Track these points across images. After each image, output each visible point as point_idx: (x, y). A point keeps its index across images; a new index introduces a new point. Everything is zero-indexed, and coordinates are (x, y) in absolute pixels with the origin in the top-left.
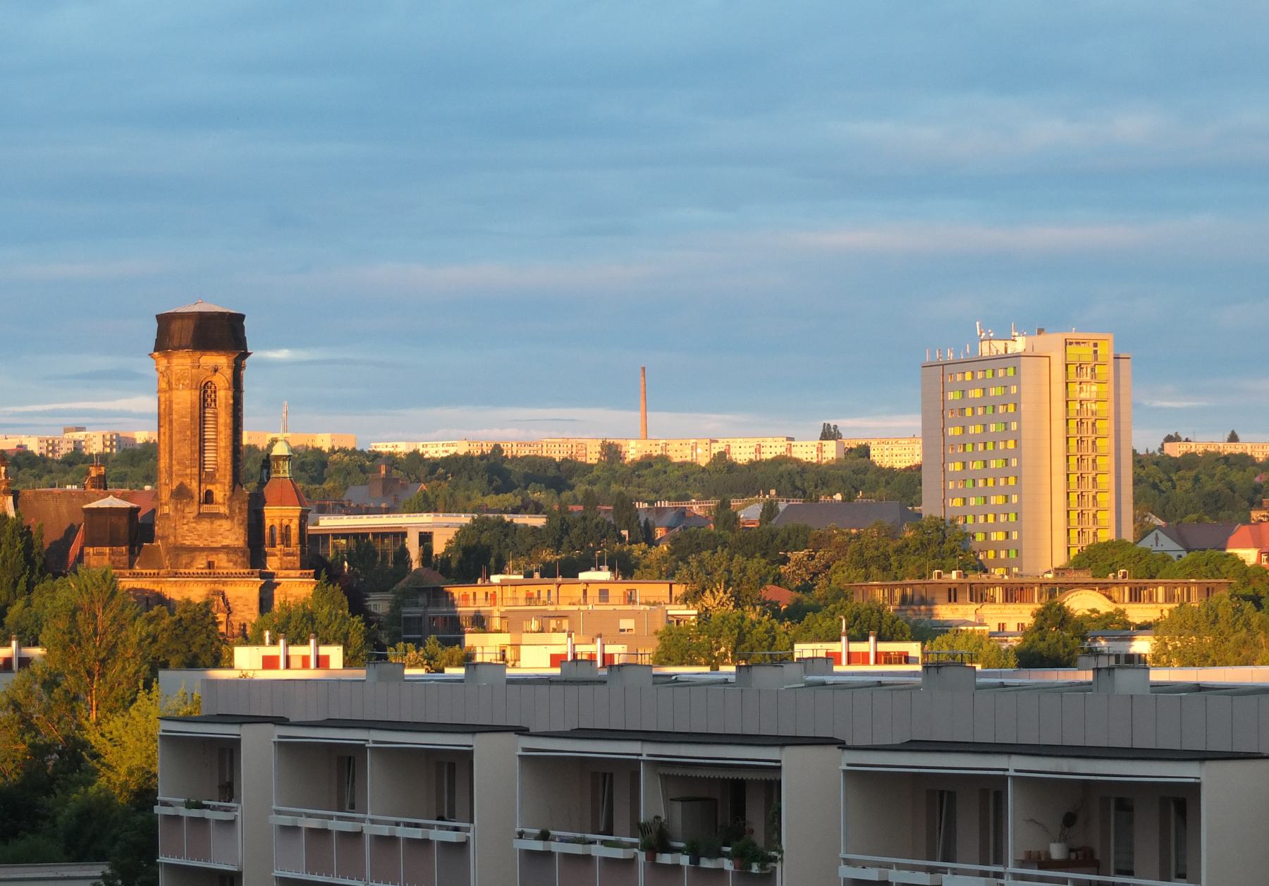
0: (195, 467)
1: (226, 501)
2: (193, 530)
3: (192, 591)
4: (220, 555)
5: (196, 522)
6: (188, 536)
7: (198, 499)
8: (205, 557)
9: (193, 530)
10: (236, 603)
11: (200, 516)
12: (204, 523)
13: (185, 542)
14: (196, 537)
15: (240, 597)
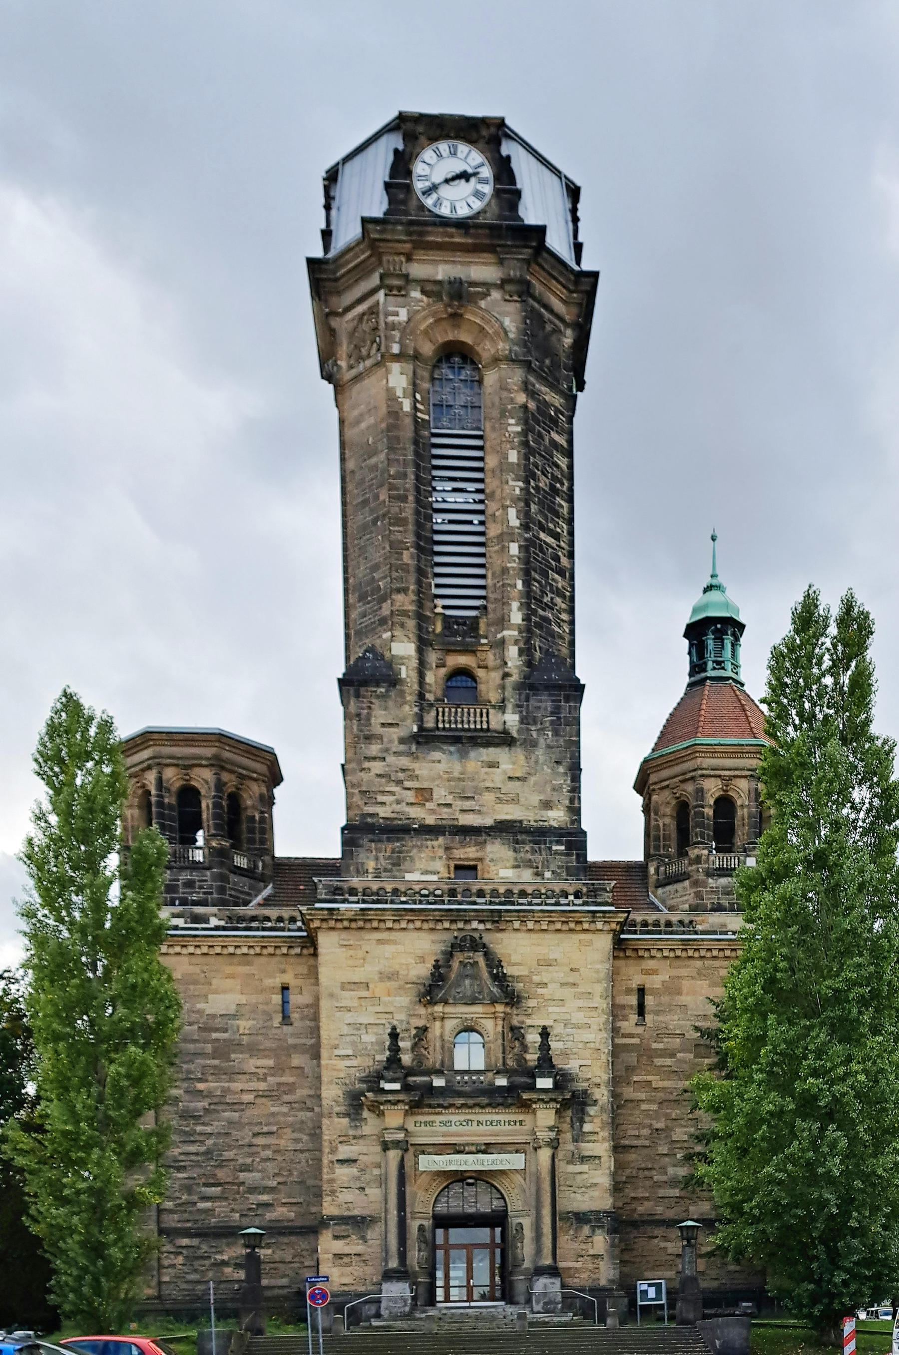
0: (405, 590)
1: (509, 692)
2: (401, 776)
3: (394, 942)
4: (489, 848)
5: (410, 754)
7: (416, 687)
8: (441, 852)
9: (401, 776)
10: (536, 979)
12: (436, 755)
14: (410, 796)
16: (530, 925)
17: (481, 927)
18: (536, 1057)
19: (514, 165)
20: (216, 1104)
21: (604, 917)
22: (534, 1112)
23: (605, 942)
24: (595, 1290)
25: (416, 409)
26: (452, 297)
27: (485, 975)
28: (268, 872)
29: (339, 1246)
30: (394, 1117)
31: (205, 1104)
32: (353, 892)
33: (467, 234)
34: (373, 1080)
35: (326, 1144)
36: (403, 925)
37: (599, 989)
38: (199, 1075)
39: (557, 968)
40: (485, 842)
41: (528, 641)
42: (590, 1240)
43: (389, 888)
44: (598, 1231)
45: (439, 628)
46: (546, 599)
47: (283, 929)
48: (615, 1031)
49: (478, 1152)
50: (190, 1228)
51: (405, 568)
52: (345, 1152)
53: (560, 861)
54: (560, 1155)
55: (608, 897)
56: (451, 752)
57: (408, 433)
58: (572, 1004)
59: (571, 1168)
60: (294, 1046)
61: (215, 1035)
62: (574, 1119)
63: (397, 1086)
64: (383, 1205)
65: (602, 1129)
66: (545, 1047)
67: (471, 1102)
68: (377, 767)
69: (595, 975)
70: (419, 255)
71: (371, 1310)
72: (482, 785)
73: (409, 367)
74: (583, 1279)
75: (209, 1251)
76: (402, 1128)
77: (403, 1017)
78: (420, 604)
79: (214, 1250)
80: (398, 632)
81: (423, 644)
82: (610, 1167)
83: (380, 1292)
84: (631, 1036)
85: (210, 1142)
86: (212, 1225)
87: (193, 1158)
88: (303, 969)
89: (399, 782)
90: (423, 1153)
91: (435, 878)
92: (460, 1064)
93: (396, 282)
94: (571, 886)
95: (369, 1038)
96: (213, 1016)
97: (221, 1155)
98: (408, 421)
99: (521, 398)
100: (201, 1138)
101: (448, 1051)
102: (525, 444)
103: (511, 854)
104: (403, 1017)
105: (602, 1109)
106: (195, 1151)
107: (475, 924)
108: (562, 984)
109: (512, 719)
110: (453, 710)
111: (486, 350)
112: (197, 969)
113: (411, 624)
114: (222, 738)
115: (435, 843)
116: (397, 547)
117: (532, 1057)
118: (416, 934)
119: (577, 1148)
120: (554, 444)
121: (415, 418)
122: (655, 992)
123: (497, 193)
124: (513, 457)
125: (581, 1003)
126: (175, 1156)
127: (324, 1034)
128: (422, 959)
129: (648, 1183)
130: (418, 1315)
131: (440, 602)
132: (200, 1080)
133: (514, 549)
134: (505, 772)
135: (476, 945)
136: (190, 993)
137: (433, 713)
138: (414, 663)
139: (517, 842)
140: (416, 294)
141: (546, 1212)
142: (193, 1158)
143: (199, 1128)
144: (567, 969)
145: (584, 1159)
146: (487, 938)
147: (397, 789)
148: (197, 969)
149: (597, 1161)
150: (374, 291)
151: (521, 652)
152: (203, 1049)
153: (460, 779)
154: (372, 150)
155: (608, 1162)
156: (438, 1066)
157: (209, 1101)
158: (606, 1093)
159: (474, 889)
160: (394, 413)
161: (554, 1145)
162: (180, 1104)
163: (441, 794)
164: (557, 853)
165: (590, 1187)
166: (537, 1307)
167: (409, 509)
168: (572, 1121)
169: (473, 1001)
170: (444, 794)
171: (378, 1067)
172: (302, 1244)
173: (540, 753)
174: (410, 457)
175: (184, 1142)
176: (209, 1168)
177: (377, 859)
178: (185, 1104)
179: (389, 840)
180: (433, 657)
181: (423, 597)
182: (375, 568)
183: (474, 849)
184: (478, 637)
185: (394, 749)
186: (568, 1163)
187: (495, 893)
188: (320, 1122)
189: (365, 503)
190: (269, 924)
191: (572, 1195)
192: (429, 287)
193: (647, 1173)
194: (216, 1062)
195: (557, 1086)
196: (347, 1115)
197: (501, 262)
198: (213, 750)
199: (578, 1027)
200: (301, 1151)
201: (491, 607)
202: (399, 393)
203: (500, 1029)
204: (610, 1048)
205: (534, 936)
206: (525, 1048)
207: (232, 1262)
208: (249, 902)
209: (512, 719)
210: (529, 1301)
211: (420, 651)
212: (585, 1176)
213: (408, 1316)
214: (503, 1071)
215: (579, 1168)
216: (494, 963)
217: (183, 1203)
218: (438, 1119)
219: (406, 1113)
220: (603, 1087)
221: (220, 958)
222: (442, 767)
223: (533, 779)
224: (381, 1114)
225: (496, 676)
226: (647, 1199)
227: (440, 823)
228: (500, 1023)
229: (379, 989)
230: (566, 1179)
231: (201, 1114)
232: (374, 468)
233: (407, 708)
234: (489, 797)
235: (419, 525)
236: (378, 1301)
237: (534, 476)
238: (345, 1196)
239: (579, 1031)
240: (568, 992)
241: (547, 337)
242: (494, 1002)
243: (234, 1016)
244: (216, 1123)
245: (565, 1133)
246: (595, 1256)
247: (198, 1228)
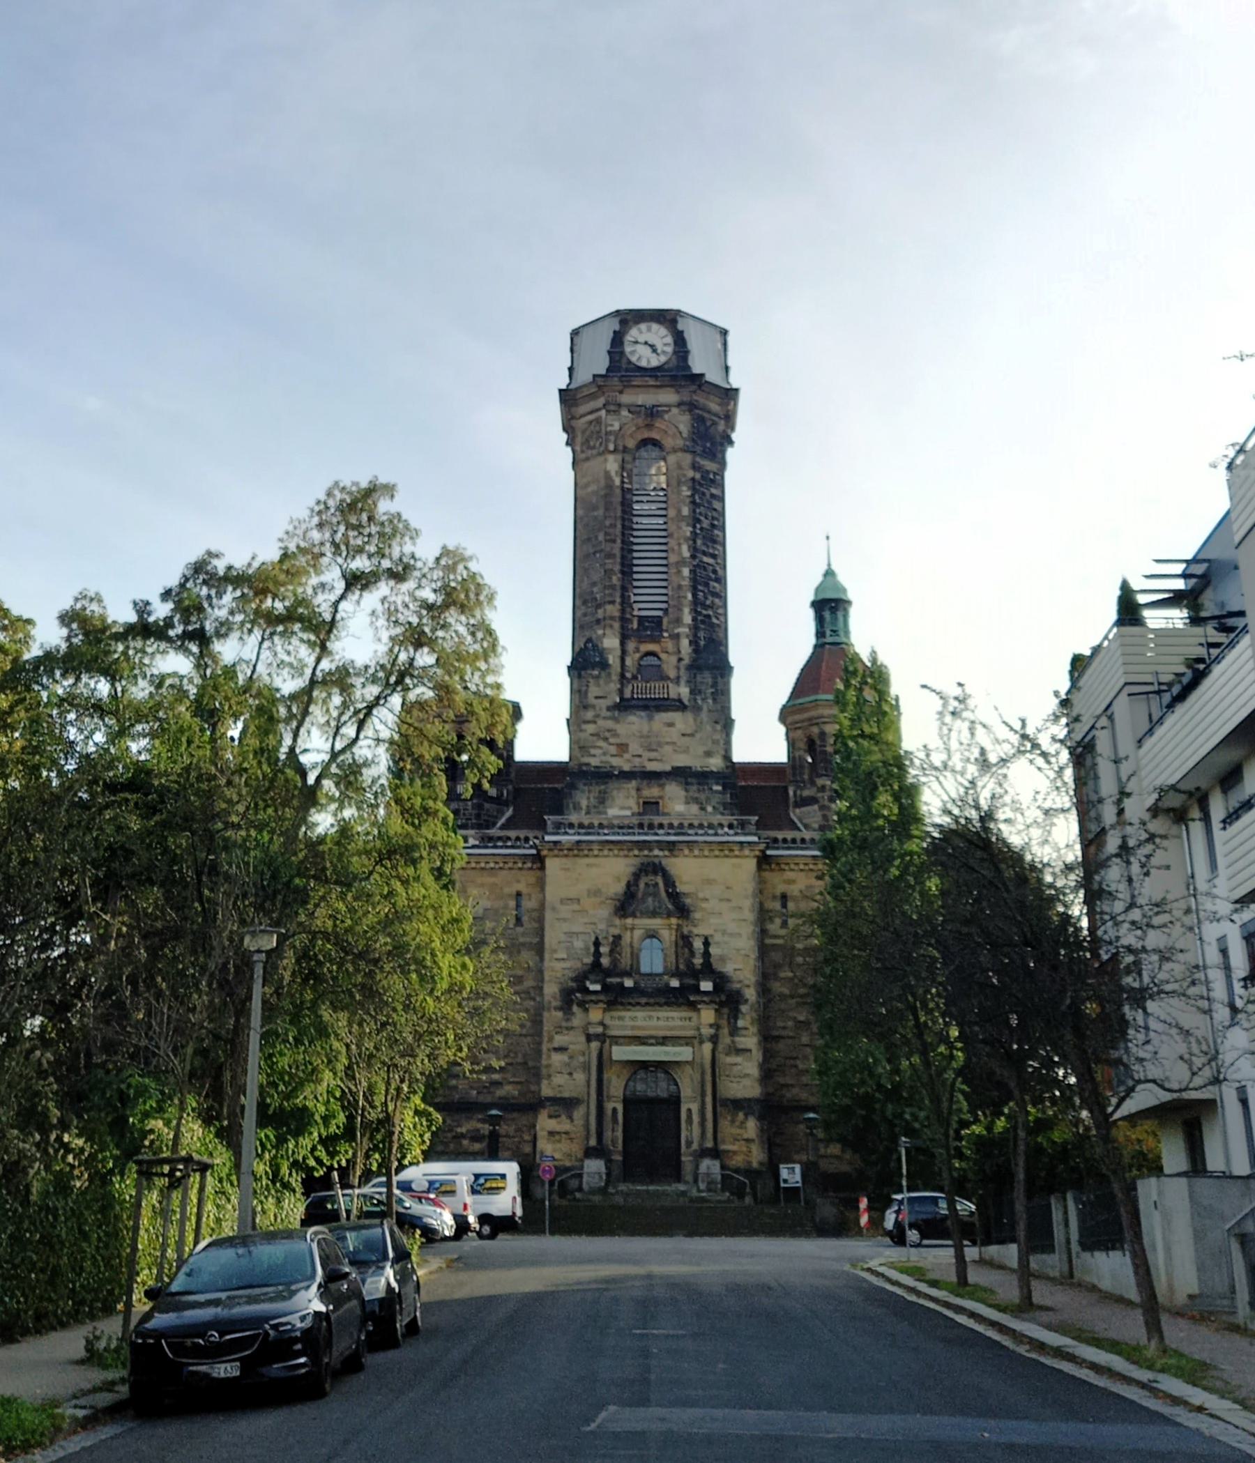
0: (613, 602)
1: (682, 672)
2: (607, 734)
5: (616, 720)
6: (595, 747)
7: (619, 670)
8: (633, 793)
9: (607, 734)
10: (701, 895)
11: (624, 706)
12: (632, 718)
13: (586, 760)
14: (613, 750)
16: (696, 852)
17: (661, 853)
18: (701, 961)
19: (686, 335)
22: (698, 1010)
23: (751, 864)
24: (748, 1172)
25: (623, 482)
26: (647, 415)
27: (663, 894)
28: (511, 798)
29: (552, 1124)
30: (596, 1014)
32: (571, 826)
33: (656, 377)
34: (580, 979)
35: (545, 1034)
36: (606, 852)
37: (747, 903)
41: (695, 635)
43: (596, 823)
45: (635, 626)
46: (708, 602)
47: (518, 847)
48: (763, 933)
49: (658, 1044)
51: (613, 587)
52: (559, 1040)
53: (716, 799)
54: (720, 1047)
57: (617, 498)
59: (730, 1060)
60: (523, 944)
63: (598, 987)
64: (586, 1090)
66: (706, 954)
67: (652, 1001)
68: (590, 728)
70: (627, 390)
71: (574, 1183)
73: (619, 457)
74: (737, 1161)
76: (602, 1023)
77: (602, 926)
78: (623, 611)
80: (608, 631)
81: (624, 639)
83: (582, 1167)
84: (776, 937)
88: (532, 880)
89: (606, 739)
90: (617, 1044)
91: (628, 813)
92: (645, 969)
93: (612, 408)
94: (726, 819)
95: (578, 944)
98: (618, 492)
99: (691, 474)
101: (635, 956)
102: (693, 502)
104: (602, 926)
105: (752, 1007)
107: (656, 852)
109: (684, 691)
111: (668, 442)
115: (630, 786)
116: (609, 573)
117: (698, 961)
118: (614, 860)
119: (733, 1042)
120: (713, 496)
121: (623, 489)
122: (795, 899)
123: (675, 352)
124: (686, 511)
127: (547, 940)
128: (619, 879)
129: (793, 1070)
130: (611, 1190)
131: (636, 606)
133: (686, 572)
135: (656, 869)
137: (630, 687)
138: (619, 653)
139: (687, 784)
140: (625, 413)
141: (709, 1099)
146: (664, 862)
150: (598, 410)
151: (691, 642)
154: (600, 323)
155: (757, 1055)
156: (628, 968)
159: (656, 823)
160: (609, 486)
161: (714, 1039)
163: (634, 747)
164: (717, 792)
166: (702, 1186)
167: (617, 548)
169: (654, 914)
171: (586, 968)
172: (524, 1120)
173: (704, 715)
174: (619, 513)
177: (588, 798)
179: (597, 784)
181: (626, 604)
182: (594, 584)
184: (661, 631)
186: (727, 1054)
187: (671, 826)
188: (541, 1015)
189: (589, 539)
190: (509, 844)
192: (632, 409)
193: (792, 1062)
195: (718, 988)
196: (560, 1009)
197: (678, 392)
199: (731, 935)
200: (525, 1036)
201: (670, 610)
202: (613, 474)
203: (673, 938)
205: (699, 860)
206: (692, 954)
208: (494, 824)
209: (684, 691)
210: (696, 1181)
211: (622, 644)
213: (603, 1191)
214: (677, 974)
216: (669, 882)
218: (627, 1014)
219: (605, 1010)
222: (635, 728)
223: (698, 736)
224: (586, 1010)
225: (674, 659)
226: (792, 1086)
228: (674, 933)
229: (587, 902)
232: (596, 518)
234: (668, 749)
235: (623, 557)
236: (580, 1176)
237: (699, 521)
238: (559, 1080)
240: (725, 905)
241: (707, 429)
242: (669, 915)
246: (748, 1140)
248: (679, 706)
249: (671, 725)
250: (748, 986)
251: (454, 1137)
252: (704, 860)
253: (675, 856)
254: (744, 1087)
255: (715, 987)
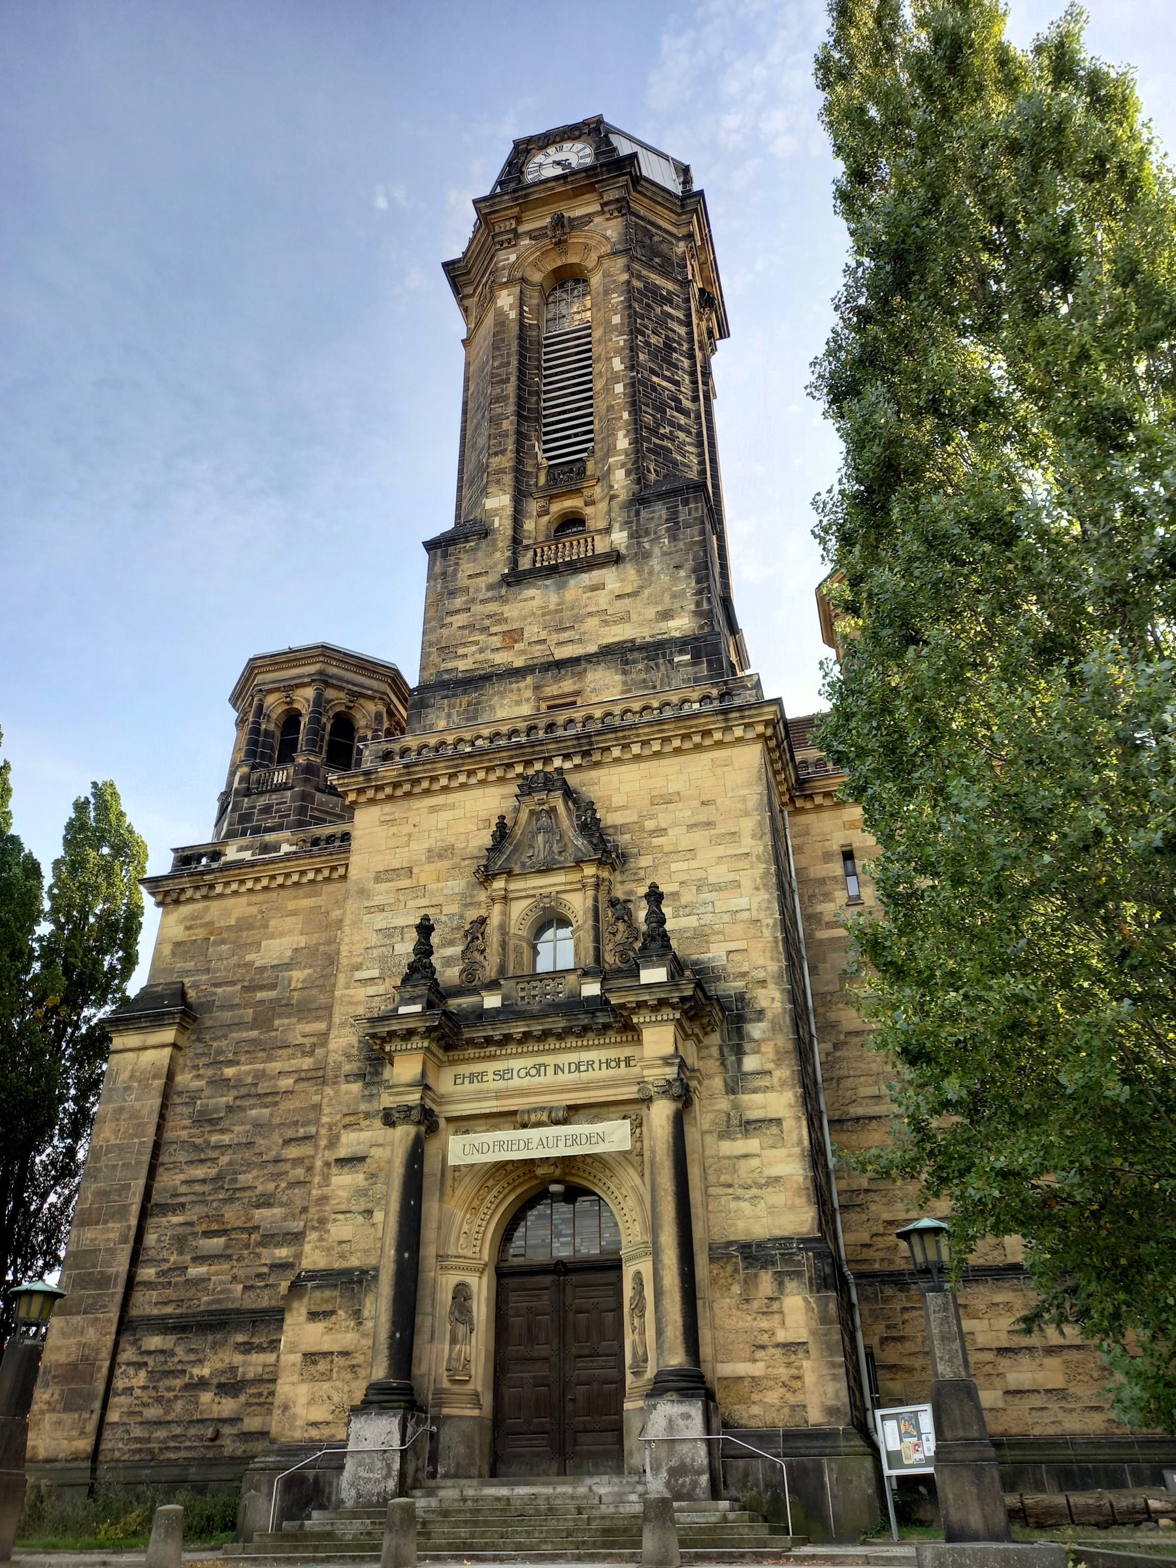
4: (590, 676)
12: (531, 592)
15: (668, 800)
20: (242, 1097)
21: (743, 717)
31: (228, 1099)
37: (748, 825)
38: (230, 1056)
39: (680, 805)
40: (585, 671)
42: (775, 1306)
44: (791, 1285)
50: (170, 1316)
55: (751, 696)
56: (547, 586)
58: (707, 855)
59: (728, 1147)
61: (260, 995)
62: (726, 1050)
65: (778, 1063)
69: (740, 806)
72: (584, 611)
75: (185, 1359)
79: (192, 1357)
81: (520, 496)
82: (800, 1142)
85: (224, 1160)
86: (202, 1308)
87: (198, 1188)
96: (262, 969)
97: (235, 1180)
100: (214, 1155)
103: (618, 678)
105: (775, 1027)
106: (202, 1176)
108: (691, 827)
110: (553, 547)
112: (254, 910)
113: (508, 479)
114: (325, 652)
119: (736, 1106)
125: (721, 851)
126: (175, 1188)
132: (230, 1063)
134: (611, 592)
136: (242, 941)
137: (530, 554)
142: (198, 1188)
143: (215, 1138)
144: (697, 803)
145: (749, 1126)
147: (481, 637)
148: (254, 910)
149: (774, 1130)
152: (242, 1017)
153: (557, 611)
155: (796, 1131)
157: (234, 1093)
158: (777, 995)
162: (199, 1102)
163: (533, 631)
165: (767, 1185)
168: (722, 1054)
170: (536, 630)
175: (192, 1162)
176: (215, 1205)
178: (205, 1101)
180: (533, 506)
183: (570, 681)
185: (481, 597)
186: (722, 1136)
191: (733, 1205)
194: (254, 1034)
198: (317, 667)
204: (777, 916)
207: (215, 1381)
212: (755, 1162)
215: (740, 1146)
217: (170, 1269)
220: (771, 986)
221: (283, 893)
227: (531, 663)
230: (719, 1171)
231: (222, 1115)
233: (498, 554)
239: (722, 895)
240: (699, 838)
243: (288, 966)
244: (237, 1128)
245: (710, 1077)
247: (181, 1316)
248: (614, 558)
249: (595, 588)
250: (763, 983)
251: (186, 1387)
252: (654, 763)
253: (597, 765)
254: (771, 1208)
255: (671, 975)
